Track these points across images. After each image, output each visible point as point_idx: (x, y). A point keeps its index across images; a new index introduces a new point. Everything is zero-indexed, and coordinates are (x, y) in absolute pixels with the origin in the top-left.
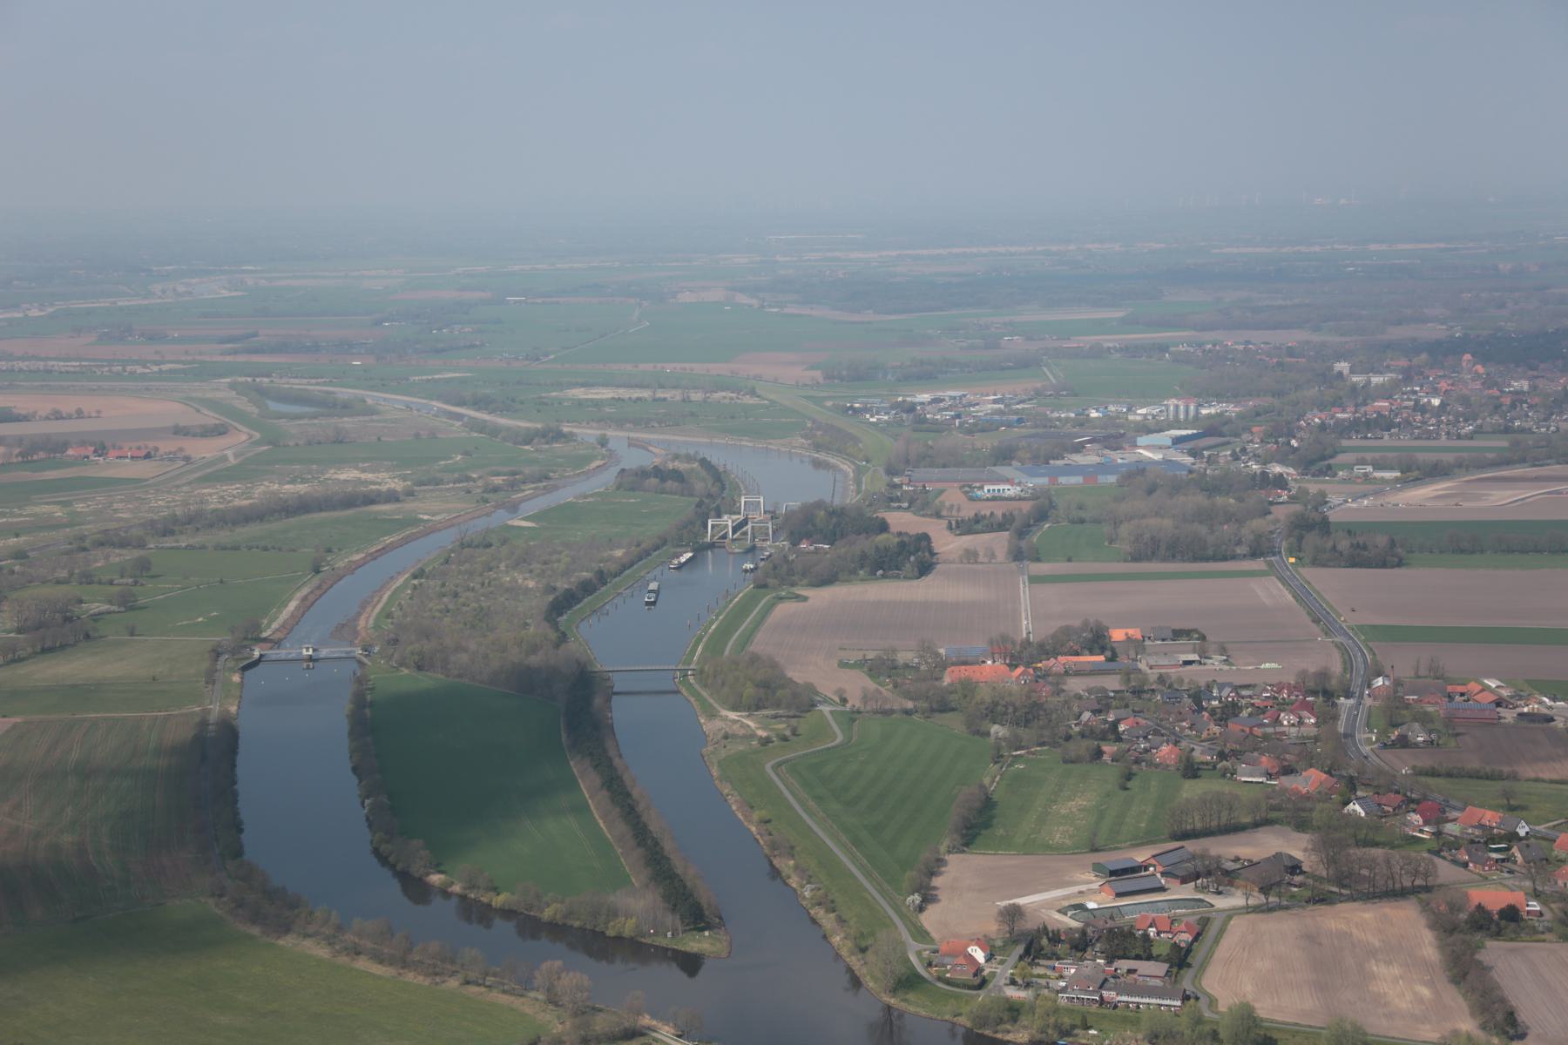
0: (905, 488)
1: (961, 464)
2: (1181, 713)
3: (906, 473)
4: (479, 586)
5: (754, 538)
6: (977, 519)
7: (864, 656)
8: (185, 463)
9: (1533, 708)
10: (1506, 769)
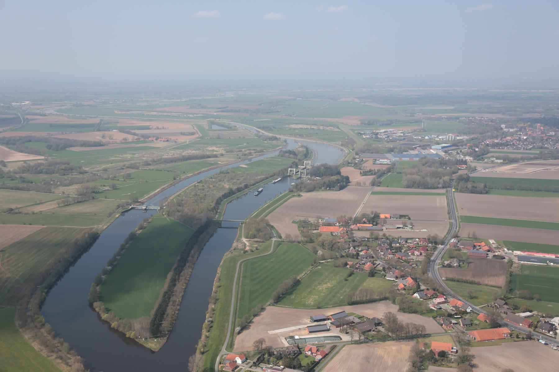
0: (357, 159)
1: (378, 153)
2: (382, 249)
3: (360, 155)
4: (213, 187)
5: (301, 175)
6: (370, 171)
7: (300, 219)
8: (175, 143)
9: (499, 254)
10: (477, 280)
